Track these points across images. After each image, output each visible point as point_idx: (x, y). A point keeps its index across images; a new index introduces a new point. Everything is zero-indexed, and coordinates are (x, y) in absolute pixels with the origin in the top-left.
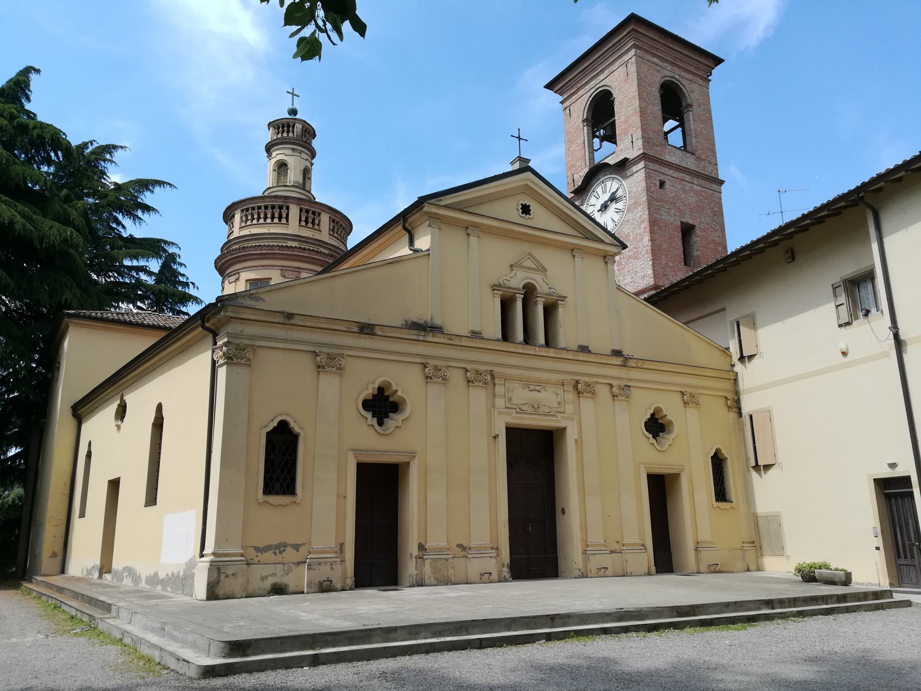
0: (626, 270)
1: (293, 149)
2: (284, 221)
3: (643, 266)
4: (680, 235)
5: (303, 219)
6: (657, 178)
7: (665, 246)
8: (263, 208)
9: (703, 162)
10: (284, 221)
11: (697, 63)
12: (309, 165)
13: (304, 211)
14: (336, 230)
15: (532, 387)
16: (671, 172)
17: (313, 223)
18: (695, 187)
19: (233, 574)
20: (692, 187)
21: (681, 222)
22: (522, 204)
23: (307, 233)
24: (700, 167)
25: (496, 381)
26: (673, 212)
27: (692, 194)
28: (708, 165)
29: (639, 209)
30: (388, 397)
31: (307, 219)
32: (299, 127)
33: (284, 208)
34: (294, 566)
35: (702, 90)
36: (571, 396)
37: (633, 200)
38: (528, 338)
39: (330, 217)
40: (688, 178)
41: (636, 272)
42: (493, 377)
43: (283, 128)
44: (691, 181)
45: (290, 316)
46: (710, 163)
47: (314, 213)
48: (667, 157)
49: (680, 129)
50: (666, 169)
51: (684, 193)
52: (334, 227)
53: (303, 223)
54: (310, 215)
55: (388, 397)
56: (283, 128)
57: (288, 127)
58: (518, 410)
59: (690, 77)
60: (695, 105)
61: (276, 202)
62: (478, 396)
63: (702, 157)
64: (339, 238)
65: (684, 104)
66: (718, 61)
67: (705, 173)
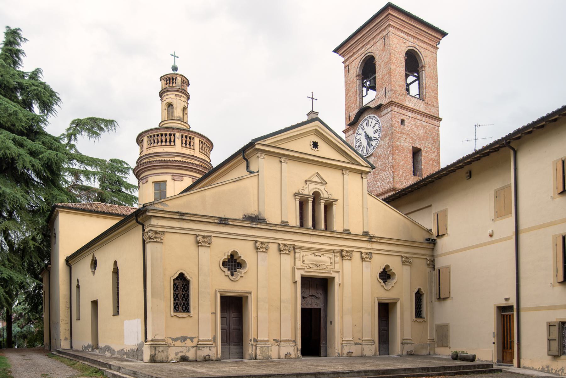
0: (378, 177)
2: (172, 143)
3: (388, 175)
4: (412, 156)
5: (184, 142)
6: (400, 118)
7: (402, 163)
8: (160, 135)
9: (429, 106)
10: (172, 143)
11: (430, 36)
12: (186, 105)
13: (184, 137)
14: (203, 148)
15: (316, 254)
16: (408, 113)
17: (190, 145)
18: (423, 123)
19: (162, 351)
20: (421, 123)
21: (413, 147)
22: (313, 142)
23: (186, 151)
24: (427, 110)
25: (296, 251)
26: (408, 140)
27: (421, 128)
28: (432, 108)
29: (388, 138)
30: (236, 260)
31: (186, 141)
33: (173, 135)
34: (191, 348)
35: (432, 56)
36: (338, 259)
37: (384, 132)
38: (314, 226)
39: (200, 140)
40: (419, 117)
41: (384, 179)
42: (294, 249)
43: (170, 80)
44: (421, 119)
45: (182, 214)
46: (434, 106)
47: (190, 138)
48: (407, 103)
49: (417, 82)
50: (406, 111)
51: (416, 127)
52: (202, 147)
53: (184, 145)
54: (188, 139)
55: (236, 260)
56: (170, 80)
57: (173, 79)
58: (308, 267)
59: (425, 46)
60: (427, 66)
61: (168, 131)
62: (287, 260)
63: (429, 103)
64: (206, 154)
65: (420, 66)
66: (444, 34)
67: (430, 113)
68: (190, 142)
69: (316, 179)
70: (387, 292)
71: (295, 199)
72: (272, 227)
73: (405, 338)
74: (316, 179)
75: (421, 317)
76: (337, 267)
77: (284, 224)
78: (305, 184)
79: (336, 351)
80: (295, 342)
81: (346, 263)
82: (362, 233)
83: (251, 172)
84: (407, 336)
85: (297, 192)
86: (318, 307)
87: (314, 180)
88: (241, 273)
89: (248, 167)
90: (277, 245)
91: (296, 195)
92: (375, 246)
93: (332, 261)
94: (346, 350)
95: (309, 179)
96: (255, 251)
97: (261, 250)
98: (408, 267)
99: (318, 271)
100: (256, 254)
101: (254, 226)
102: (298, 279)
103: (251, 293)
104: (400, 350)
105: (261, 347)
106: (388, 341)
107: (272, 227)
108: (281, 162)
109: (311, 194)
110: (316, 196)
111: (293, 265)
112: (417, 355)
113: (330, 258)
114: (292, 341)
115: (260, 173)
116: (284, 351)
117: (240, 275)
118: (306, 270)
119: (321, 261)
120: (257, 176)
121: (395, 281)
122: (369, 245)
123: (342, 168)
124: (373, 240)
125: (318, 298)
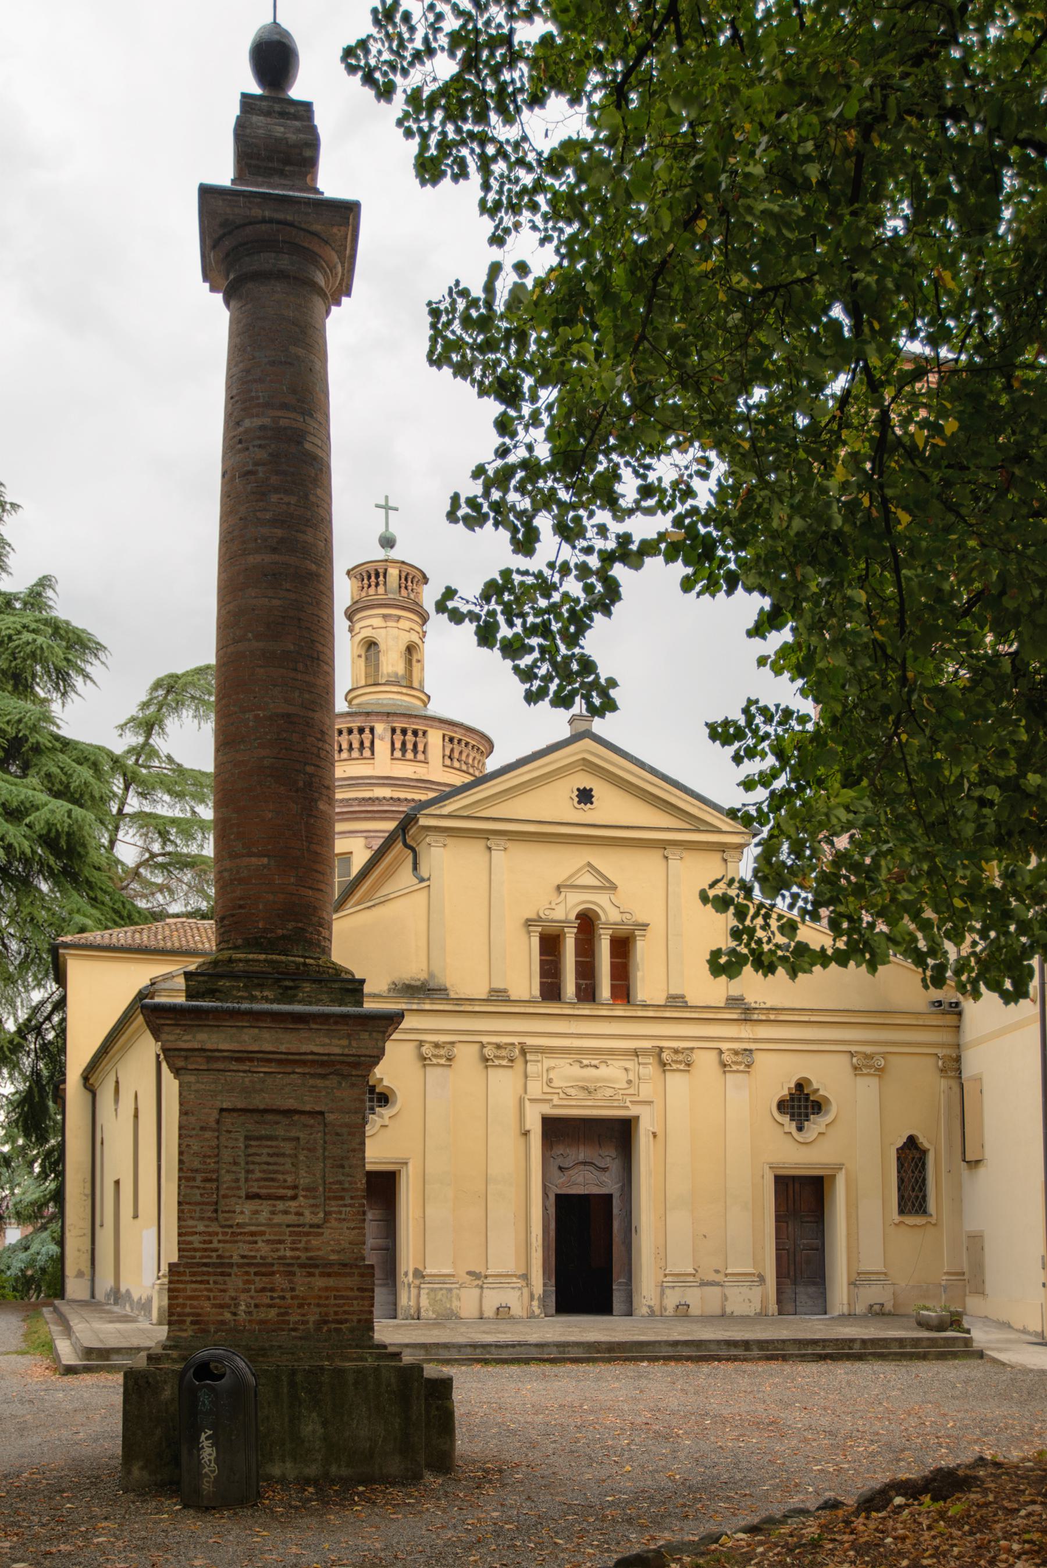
1: (385, 617)
2: (367, 753)
5: (398, 745)
10: (367, 753)
13: (398, 732)
14: (456, 755)
15: (586, 1062)
23: (405, 770)
25: (529, 1057)
31: (404, 744)
32: (393, 572)
33: (367, 731)
36: (649, 1069)
38: (587, 993)
42: (523, 1052)
47: (415, 733)
52: (452, 750)
53: (398, 754)
54: (410, 737)
58: (562, 1095)
64: (464, 767)
68: (415, 745)
69: (588, 880)
70: (804, 1148)
71: (529, 932)
72: (463, 1006)
73: (863, 1268)
74: (588, 880)
75: (925, 1212)
76: (646, 1091)
77: (498, 996)
78: (556, 894)
79: (644, 1301)
80: (526, 1277)
81: (676, 1082)
82: (724, 1000)
83: (422, 880)
84: (872, 1261)
85: (533, 916)
86: (604, 1191)
87: (580, 882)
88: (381, 1116)
89: (415, 867)
90: (477, 1047)
91: (529, 923)
92: (764, 1032)
93: (631, 1077)
94: (672, 1300)
95: (571, 877)
96: (420, 1064)
97: (435, 1061)
98: (874, 1082)
99: (589, 1103)
100: (421, 1072)
101: (415, 1007)
102: (535, 1127)
103: (406, 1163)
104: (845, 1301)
105: (432, 1289)
106: (823, 1277)
107: (463, 1006)
108: (489, 849)
109: (572, 916)
110: (587, 922)
111: (521, 1091)
112: (902, 1316)
113: (626, 1069)
114: (519, 1277)
115: (432, 883)
116: (492, 1299)
117: (379, 1122)
118: (556, 1102)
119: (598, 1080)
120: (425, 891)
121: (829, 1118)
122: (745, 1031)
123: (663, 845)
124: (755, 1017)
125: (605, 1170)
